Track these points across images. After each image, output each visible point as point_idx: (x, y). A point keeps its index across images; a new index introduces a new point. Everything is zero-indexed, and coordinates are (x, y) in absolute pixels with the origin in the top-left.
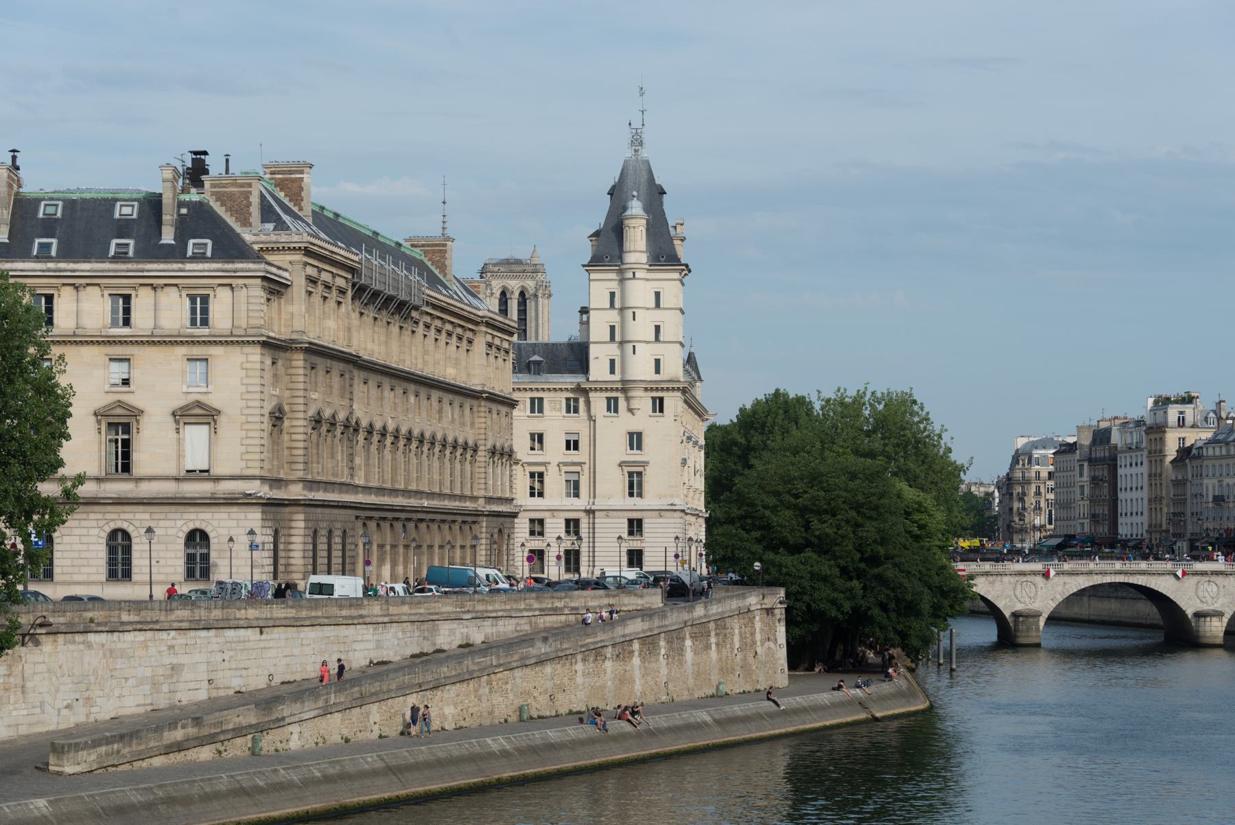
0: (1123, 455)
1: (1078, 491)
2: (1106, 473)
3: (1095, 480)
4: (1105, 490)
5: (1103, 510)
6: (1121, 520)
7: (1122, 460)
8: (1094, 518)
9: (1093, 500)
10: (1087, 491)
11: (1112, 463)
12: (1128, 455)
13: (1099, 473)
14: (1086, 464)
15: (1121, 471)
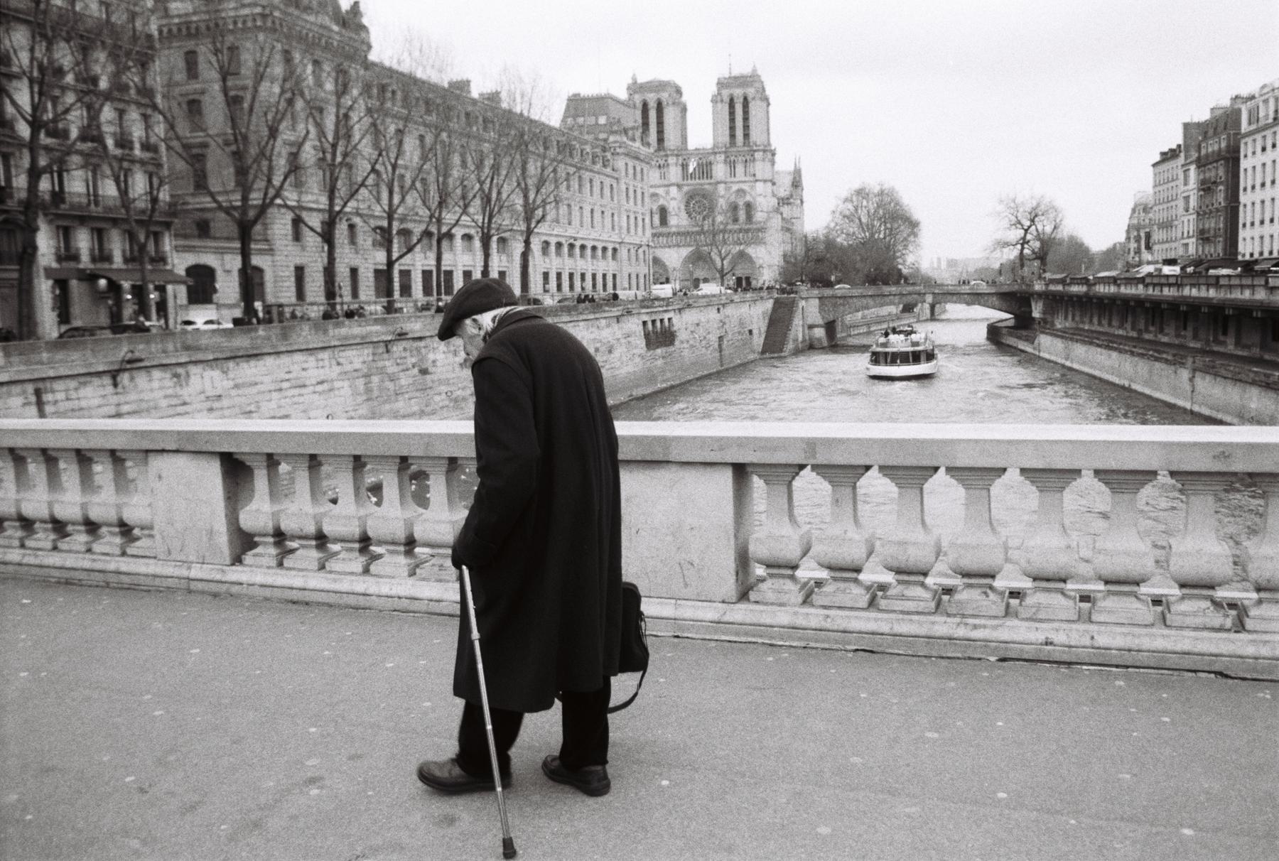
0: (1249, 140)
1: (1181, 203)
2: (1221, 172)
3: (1206, 188)
4: (1220, 197)
5: (1216, 223)
6: (1242, 234)
7: (1246, 148)
8: (1204, 237)
9: (1201, 214)
10: (1193, 203)
11: (1232, 159)
12: (1258, 137)
13: (1211, 174)
14: (1193, 167)
15: (1244, 164)
